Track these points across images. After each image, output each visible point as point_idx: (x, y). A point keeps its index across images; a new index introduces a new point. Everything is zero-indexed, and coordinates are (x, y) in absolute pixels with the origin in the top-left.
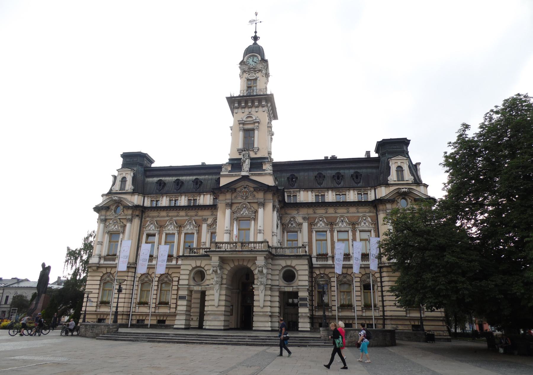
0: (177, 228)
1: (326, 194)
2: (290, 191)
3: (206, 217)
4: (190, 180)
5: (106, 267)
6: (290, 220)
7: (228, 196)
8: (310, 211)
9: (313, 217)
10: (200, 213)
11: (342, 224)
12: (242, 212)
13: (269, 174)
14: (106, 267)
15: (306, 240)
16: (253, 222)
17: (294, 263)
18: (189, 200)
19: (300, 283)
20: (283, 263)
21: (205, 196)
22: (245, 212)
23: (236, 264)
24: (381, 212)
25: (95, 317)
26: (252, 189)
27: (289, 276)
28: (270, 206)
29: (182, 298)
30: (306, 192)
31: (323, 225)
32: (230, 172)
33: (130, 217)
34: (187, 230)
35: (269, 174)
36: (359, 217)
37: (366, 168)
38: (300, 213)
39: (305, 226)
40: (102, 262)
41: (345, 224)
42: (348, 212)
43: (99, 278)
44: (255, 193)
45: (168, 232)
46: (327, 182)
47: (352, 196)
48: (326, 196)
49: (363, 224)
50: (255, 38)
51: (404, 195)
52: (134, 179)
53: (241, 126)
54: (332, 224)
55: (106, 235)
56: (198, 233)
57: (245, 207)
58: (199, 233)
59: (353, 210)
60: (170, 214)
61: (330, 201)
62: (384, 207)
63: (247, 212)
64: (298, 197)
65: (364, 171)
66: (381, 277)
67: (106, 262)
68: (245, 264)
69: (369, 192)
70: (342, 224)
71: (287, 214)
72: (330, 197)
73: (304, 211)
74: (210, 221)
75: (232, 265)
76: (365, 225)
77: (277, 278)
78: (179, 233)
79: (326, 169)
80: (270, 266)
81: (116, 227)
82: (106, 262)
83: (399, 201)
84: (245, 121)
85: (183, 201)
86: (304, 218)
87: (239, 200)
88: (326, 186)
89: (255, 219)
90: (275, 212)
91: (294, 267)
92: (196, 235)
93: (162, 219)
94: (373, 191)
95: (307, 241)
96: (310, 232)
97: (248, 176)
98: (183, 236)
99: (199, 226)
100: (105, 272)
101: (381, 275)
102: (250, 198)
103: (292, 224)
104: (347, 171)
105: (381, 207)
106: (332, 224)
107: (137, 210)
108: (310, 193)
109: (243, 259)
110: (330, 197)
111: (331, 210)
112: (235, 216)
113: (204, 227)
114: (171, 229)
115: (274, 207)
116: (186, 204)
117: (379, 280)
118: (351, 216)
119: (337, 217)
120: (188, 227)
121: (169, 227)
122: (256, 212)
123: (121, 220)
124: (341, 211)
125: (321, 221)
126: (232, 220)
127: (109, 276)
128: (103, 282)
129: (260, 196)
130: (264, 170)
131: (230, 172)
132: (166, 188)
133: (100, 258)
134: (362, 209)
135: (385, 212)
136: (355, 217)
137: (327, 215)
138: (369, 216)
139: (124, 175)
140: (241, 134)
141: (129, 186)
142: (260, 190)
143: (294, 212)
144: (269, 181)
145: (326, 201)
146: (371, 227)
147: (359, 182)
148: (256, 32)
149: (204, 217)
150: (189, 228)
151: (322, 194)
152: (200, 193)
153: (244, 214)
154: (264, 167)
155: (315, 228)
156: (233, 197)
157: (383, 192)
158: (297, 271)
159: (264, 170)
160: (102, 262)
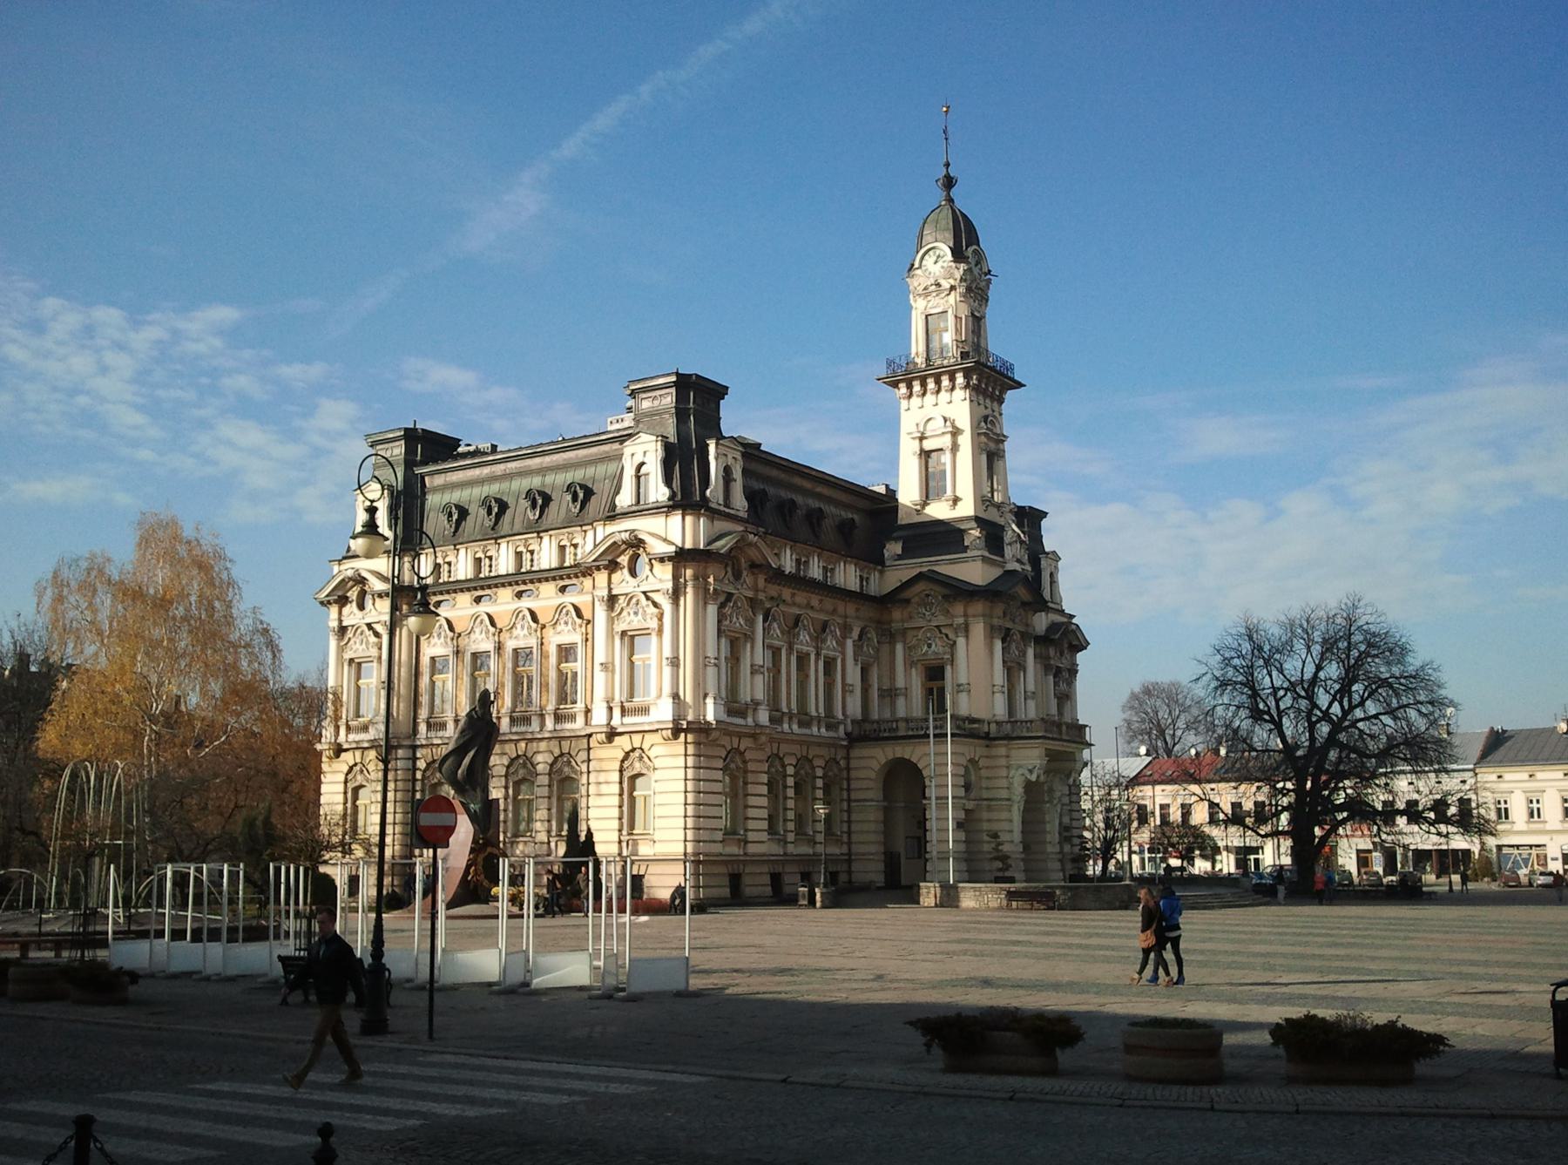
25: (722, 869)
43: (720, 764)
50: (949, 182)
53: (983, 439)
74: (855, 634)
98: (821, 664)
99: (842, 644)
113: (849, 643)
114: (804, 639)
122: (1025, 654)
139: (730, 461)
140: (984, 457)
141: (740, 503)
148: (947, 165)
157: (1041, 622)
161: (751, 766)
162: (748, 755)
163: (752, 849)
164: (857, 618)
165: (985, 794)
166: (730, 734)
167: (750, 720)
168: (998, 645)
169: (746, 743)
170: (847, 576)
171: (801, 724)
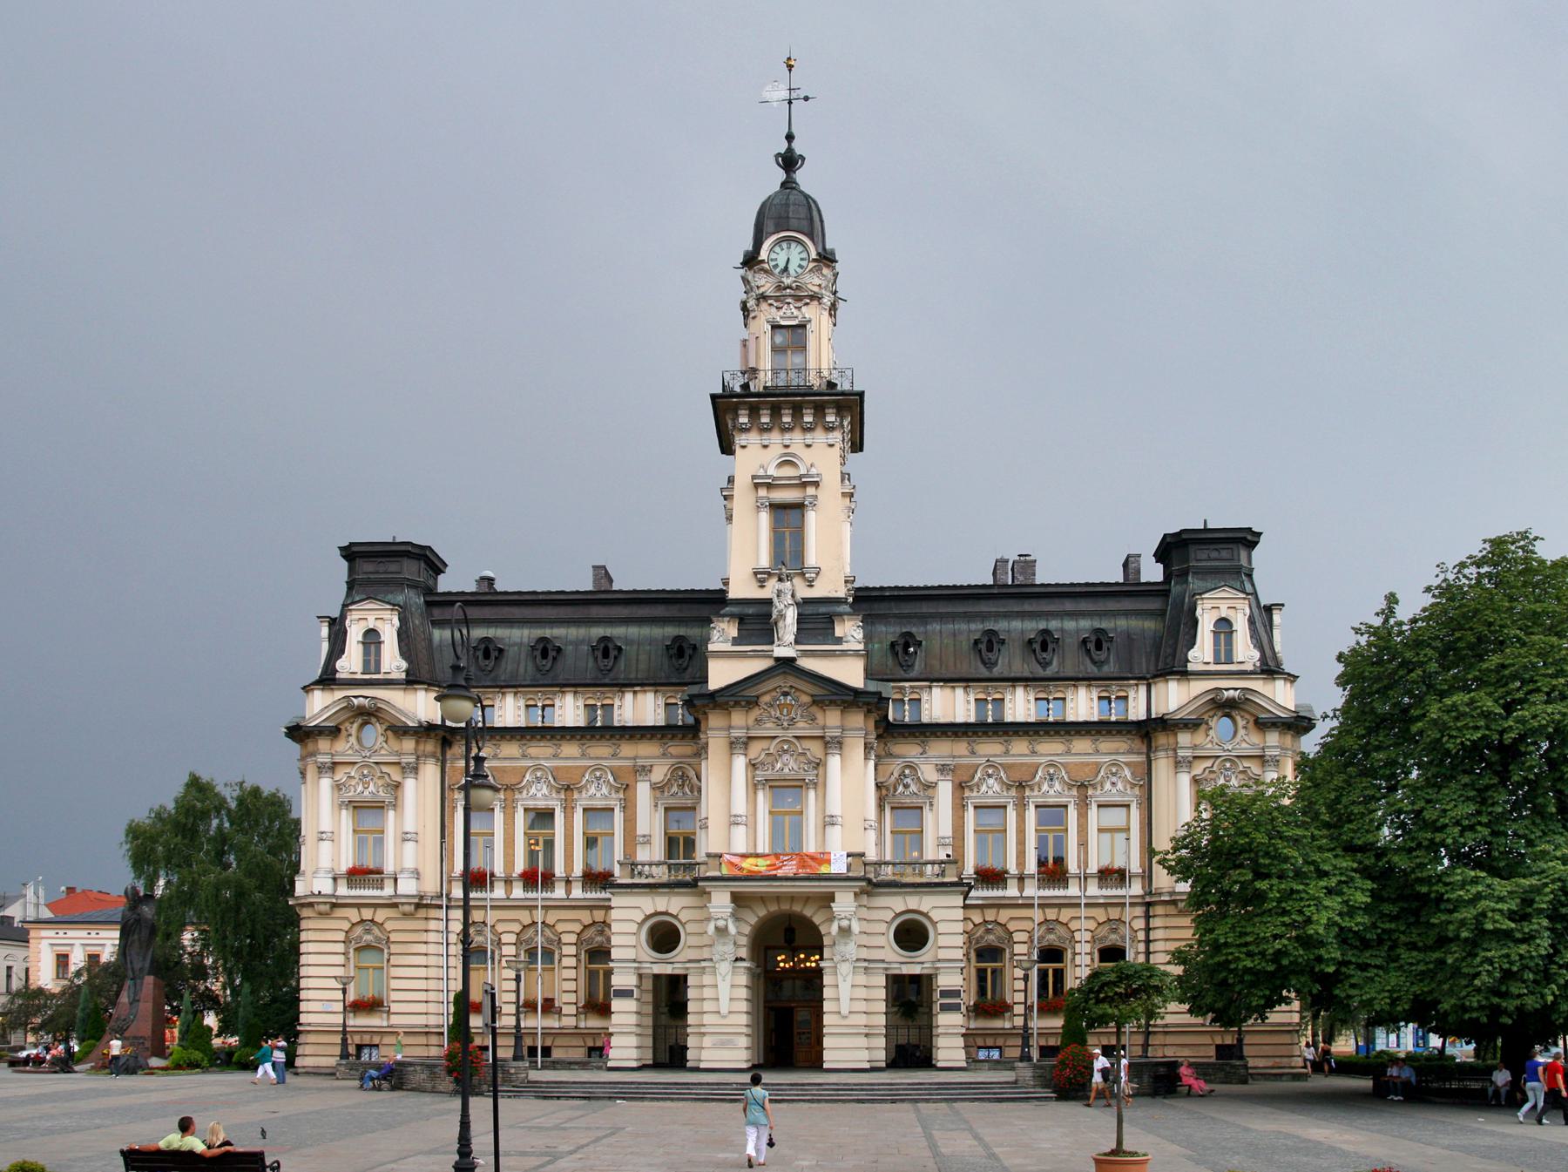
0: (558, 792)
1: (1008, 697)
2: (903, 688)
3: (647, 763)
4: (577, 643)
5: (359, 906)
6: (902, 774)
7: (738, 718)
8: (961, 747)
9: (968, 766)
10: (627, 749)
11: (1051, 786)
12: (779, 766)
13: (856, 653)
14: (359, 906)
15: (946, 830)
16: (812, 794)
17: (925, 903)
18: (590, 708)
19: (942, 954)
20: (898, 903)
21: (639, 696)
22: (788, 766)
23: (773, 908)
24: (1161, 754)
26: (806, 699)
27: (912, 935)
28: (856, 749)
29: (625, 994)
30: (948, 691)
31: (997, 787)
32: (736, 642)
33: (412, 759)
34: (592, 797)
35: (856, 653)
36: (1098, 766)
37: (1127, 614)
38: (930, 753)
39: (945, 790)
40: (343, 890)
41: (1057, 786)
42: (1068, 752)
43: (341, 936)
44: (814, 709)
45: (531, 804)
46: (1011, 660)
47: (1082, 705)
48: (1008, 705)
49: (1108, 786)
51: (1226, 707)
52: (403, 635)
54: (1021, 786)
55: (344, 812)
56: (624, 808)
57: (785, 751)
58: (629, 807)
59: (1082, 745)
60: (533, 751)
61: (1020, 718)
62: (1171, 740)
63: (792, 764)
64: (925, 706)
65: (1122, 623)
66: (1148, 929)
67: (354, 892)
68: (797, 908)
69: (1132, 694)
70: (1051, 786)
71: (890, 755)
72: (1020, 706)
73: (942, 749)
74: (659, 774)
75: (762, 912)
76: (1116, 788)
77: (881, 941)
78: (568, 810)
79: (1008, 616)
80: (864, 913)
81: (371, 788)
82: (354, 892)
83: (1212, 724)
84: (775, 478)
85: (569, 710)
86: (942, 769)
87: (769, 729)
88: (1006, 674)
89: (819, 784)
90: (872, 764)
91: (926, 915)
92: (618, 816)
93: (506, 764)
94: (1143, 690)
95: (950, 834)
96: (959, 807)
97: (793, 660)
100: (355, 919)
101: (1147, 923)
102: (801, 725)
103: (906, 786)
104: (1070, 625)
105: (1162, 739)
106: (1021, 786)
107: (428, 736)
108: (960, 692)
109: (793, 898)
110: (1020, 706)
111: (1020, 747)
112: (761, 774)
113: (643, 791)
115: (868, 747)
116: (581, 722)
117: (1141, 936)
118: (1076, 764)
119: (1037, 767)
120: (592, 790)
121: (533, 791)
122: (819, 764)
123: (385, 769)
124: (1050, 748)
125: (989, 776)
126: (754, 786)
127: (368, 931)
128: (353, 945)
129: (832, 719)
130: (839, 641)
131: (736, 642)
132: (507, 666)
133: (335, 879)
134: (1106, 745)
135: (1171, 753)
136: (1088, 764)
137: (1010, 760)
138: (1126, 764)
142: (833, 703)
143: (909, 750)
144: (851, 673)
145: (1008, 718)
146: (1132, 796)
147: (1106, 661)
149: (640, 762)
150: (597, 793)
151: (998, 696)
152: (623, 686)
153: (786, 770)
154: (839, 632)
155: (973, 798)
156: (751, 721)
158: (934, 924)
159: (839, 641)
160: (343, 890)
161: (393, 937)
162: (389, 926)
163: (395, 1020)
164: (664, 755)
165: (693, 954)
166: (334, 906)
167: (388, 890)
168: (740, 762)
169: (381, 915)
170: (641, 708)
171: (526, 888)
